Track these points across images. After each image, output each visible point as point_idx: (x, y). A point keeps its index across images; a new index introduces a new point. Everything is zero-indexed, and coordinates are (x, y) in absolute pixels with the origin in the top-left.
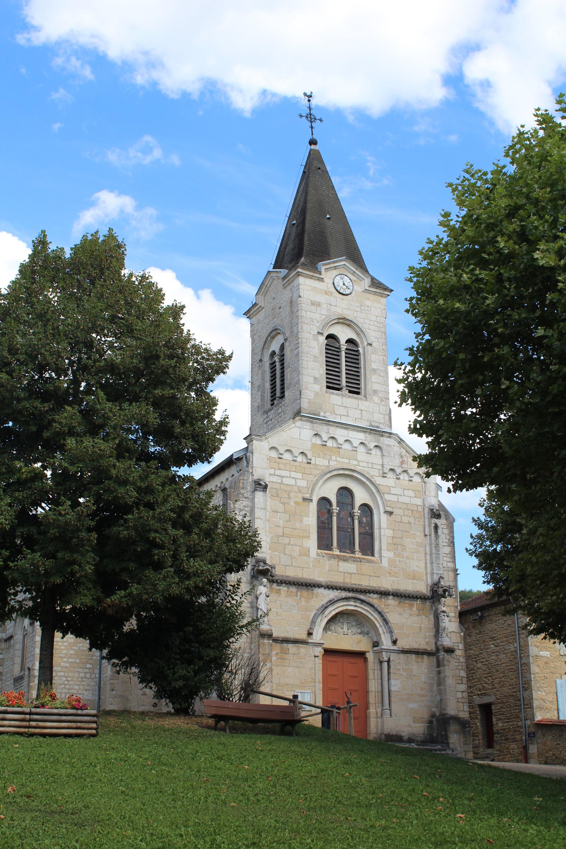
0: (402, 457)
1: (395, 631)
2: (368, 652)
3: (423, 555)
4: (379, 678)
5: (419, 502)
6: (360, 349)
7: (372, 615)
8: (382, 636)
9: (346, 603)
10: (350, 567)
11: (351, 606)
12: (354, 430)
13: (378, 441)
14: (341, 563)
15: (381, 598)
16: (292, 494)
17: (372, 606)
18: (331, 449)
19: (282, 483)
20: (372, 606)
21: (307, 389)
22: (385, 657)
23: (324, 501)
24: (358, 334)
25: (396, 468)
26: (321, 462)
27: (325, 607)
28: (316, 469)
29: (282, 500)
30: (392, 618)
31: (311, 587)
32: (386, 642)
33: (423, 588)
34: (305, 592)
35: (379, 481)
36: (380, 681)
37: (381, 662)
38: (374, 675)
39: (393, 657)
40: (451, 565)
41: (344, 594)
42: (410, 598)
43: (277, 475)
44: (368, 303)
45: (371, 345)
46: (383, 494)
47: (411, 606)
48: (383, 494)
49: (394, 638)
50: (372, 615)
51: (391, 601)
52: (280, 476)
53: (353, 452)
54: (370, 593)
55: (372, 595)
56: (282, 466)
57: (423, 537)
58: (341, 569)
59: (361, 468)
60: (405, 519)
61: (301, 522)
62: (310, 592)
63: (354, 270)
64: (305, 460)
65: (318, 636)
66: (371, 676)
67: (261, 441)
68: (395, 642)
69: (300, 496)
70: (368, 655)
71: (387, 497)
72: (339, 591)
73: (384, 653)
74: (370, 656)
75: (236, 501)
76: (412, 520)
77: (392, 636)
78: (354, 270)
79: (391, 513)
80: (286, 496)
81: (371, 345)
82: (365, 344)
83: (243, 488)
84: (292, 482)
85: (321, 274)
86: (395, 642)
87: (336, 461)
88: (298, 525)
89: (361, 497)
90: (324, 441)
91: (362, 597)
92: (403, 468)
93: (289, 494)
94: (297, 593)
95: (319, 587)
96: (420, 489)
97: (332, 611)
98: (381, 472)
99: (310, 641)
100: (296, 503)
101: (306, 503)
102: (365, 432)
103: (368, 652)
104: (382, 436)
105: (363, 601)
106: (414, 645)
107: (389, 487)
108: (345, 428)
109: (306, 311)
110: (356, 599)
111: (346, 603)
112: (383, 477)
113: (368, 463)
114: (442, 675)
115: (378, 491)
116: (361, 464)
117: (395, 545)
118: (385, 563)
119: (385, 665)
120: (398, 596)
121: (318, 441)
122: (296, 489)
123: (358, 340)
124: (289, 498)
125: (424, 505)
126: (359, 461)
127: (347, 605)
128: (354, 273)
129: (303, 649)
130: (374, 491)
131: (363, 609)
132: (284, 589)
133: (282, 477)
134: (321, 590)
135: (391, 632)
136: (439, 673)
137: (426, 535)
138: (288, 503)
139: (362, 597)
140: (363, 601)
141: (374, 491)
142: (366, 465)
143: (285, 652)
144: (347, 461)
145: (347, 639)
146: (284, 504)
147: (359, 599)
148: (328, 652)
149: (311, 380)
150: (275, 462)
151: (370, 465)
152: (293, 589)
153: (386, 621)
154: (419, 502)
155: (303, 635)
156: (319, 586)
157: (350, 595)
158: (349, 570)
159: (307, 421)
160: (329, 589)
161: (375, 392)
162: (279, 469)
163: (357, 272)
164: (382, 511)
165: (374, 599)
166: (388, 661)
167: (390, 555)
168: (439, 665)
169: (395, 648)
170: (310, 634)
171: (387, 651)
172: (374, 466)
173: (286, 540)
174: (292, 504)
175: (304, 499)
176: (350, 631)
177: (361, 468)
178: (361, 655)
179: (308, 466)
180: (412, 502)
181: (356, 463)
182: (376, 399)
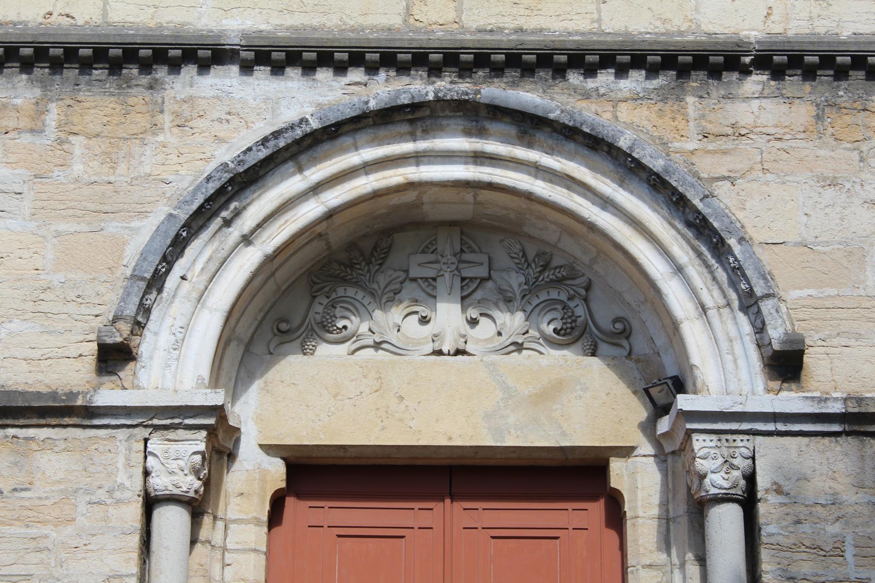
2: (626, 452)
7: (606, 203)
8: (694, 334)
9: (408, 147)
11: (446, 161)
17: (595, 144)
20: (595, 144)
22: (714, 464)
27: (244, 180)
30: (764, 209)
31: (146, 66)
32: (723, 369)
34: (97, 104)
37: (699, 507)
39: (773, 457)
41: (384, 89)
49: (776, 334)
50: (606, 203)
51: (754, 102)
54: (590, 71)
55: (605, 78)
62: (138, 97)
65: (177, 362)
68: (786, 365)
70: (619, 473)
72: (356, 75)
73: (701, 444)
74: (639, 482)
77: (760, 329)
86: (786, 365)
91: (527, 96)
94: (40, 109)
95: (204, 66)
97: (293, 206)
99: (108, 396)
103: (626, 452)
105: (529, 125)
110: (478, 116)
111: (408, 147)
119: (726, 523)
120: (809, 73)
127: (417, 158)
129: (54, 455)
131: (537, 170)
134: (225, 79)
135: (750, 303)
139: (527, 96)
140: (529, 125)
147: (498, 112)
148: (315, 474)
155: (69, 371)
157: (418, 87)
160: (278, 69)
165: (621, 107)
166: (748, 502)
169: (790, 400)
170: (114, 357)
176: (486, 327)
178: (579, 475)
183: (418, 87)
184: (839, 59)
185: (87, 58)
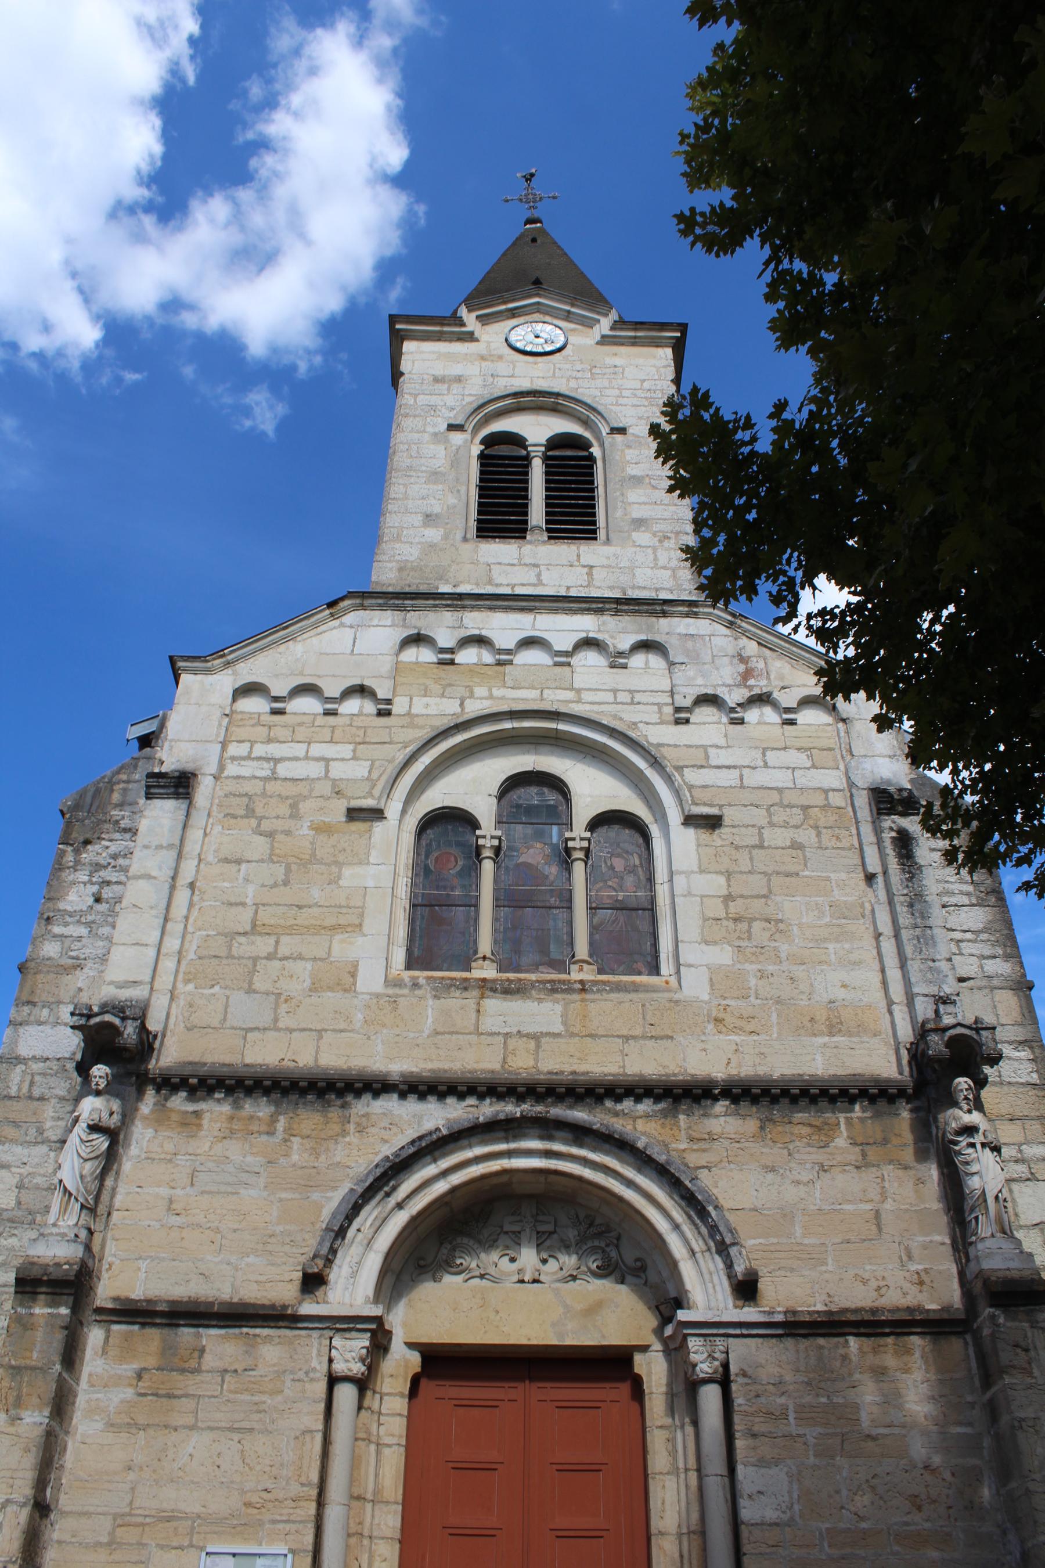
0: (743, 659)
1: (750, 1243)
2: (644, 1349)
3: (869, 941)
4: (692, 1463)
5: (833, 779)
6: (595, 451)
7: (630, 1183)
8: (687, 1270)
9: (503, 1147)
10: (541, 1014)
11: (527, 1156)
12: (555, 611)
13: (650, 629)
14: (493, 1004)
15: (671, 1113)
16: (304, 807)
17: (622, 1146)
18: (473, 670)
19: (274, 777)
20: (622, 1146)
21: (398, 539)
22: (701, 1356)
23: (448, 823)
24: (586, 423)
25: (722, 692)
26: (437, 707)
28: (412, 725)
29: (266, 826)
31: (341, 1093)
32: (707, 1294)
33: (881, 1060)
34: (309, 1118)
35: (660, 734)
36: (693, 1476)
38: (673, 1453)
39: (742, 1352)
40: (1000, 967)
41: (488, 1110)
42: (813, 1100)
43: (259, 759)
44: (618, 361)
45: (622, 431)
46: (679, 769)
47: (825, 1133)
48: (679, 769)
49: (739, 1269)
50: (630, 1183)
51: (722, 1120)
52: (267, 759)
53: (558, 669)
54: (619, 1099)
55: (627, 1104)
56: (278, 732)
57: (862, 884)
58: (489, 1023)
59: (588, 707)
60: (777, 837)
61: (334, 881)
62: (334, 1113)
63: (568, 308)
64: (370, 707)
65: (352, 1287)
66: (659, 1459)
67: (208, 671)
68: (746, 1289)
69: (340, 807)
71: (692, 776)
72: (471, 1101)
73: (693, 1343)
74: (653, 1369)
75: (87, 842)
76: (806, 836)
77: (729, 1266)
78: (568, 308)
79: (712, 823)
80: (284, 810)
81: (622, 431)
82: (604, 430)
83: (121, 805)
84: (315, 770)
85: (463, 325)
87: (491, 697)
88: (316, 894)
89: (592, 789)
90: (443, 651)
91: (579, 1115)
92: (750, 688)
93: (294, 806)
94: (273, 1120)
96: (832, 743)
97: (430, 1184)
98: (669, 710)
99: (308, 1308)
100: (322, 829)
101: (358, 826)
102: (599, 611)
103: (644, 1349)
104: (664, 614)
106: (855, 1296)
107: (705, 747)
108: (522, 610)
109: (416, 396)
110: (548, 1127)
111: (503, 1147)
112: (678, 722)
113: (615, 691)
114: (1005, 1419)
115: (655, 763)
116: (587, 696)
117: (738, 919)
118: (695, 986)
119: (710, 1397)
120: (755, 1100)
121: (426, 655)
122: (326, 788)
123: (587, 434)
124: (295, 815)
125: (851, 785)
126: (578, 691)
127: (509, 1154)
128: (568, 316)
129: (272, 1348)
130: (641, 764)
132: (216, 1111)
133: (277, 761)
134: (389, 1105)
135: (722, 1249)
136: (993, 1411)
137: (870, 878)
138: (288, 833)
139: (579, 1115)
140: (581, 1133)
141: (641, 764)
142: (609, 697)
143: (185, 1364)
144: (534, 694)
145: (522, 1298)
146: (271, 835)
147: (561, 1125)
148: (441, 1362)
149: (418, 520)
150: (259, 723)
151: (623, 697)
152: (259, 1109)
153: (695, 1204)
154: (833, 779)
156: (376, 1086)
157: (510, 1109)
158: (529, 1030)
159: (382, 607)
160: (422, 1096)
161: (639, 523)
162: (269, 741)
163: (573, 310)
164: (675, 817)
165: (640, 1122)
166: (724, 1381)
167: (723, 956)
168: (987, 1378)
169: (750, 1314)
170: (313, 1282)
171: (709, 1328)
172: (638, 697)
173: (263, 945)
174: (305, 831)
175: (354, 814)
176: (552, 1265)
177: (588, 707)
178: (613, 1364)
179: (384, 721)
180: (801, 782)
181: (570, 695)
182: (643, 537)
183: (510, 1109)
184: (773, 1091)
185: (250, 1086)
